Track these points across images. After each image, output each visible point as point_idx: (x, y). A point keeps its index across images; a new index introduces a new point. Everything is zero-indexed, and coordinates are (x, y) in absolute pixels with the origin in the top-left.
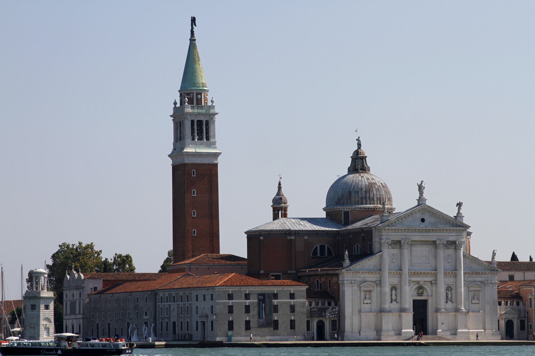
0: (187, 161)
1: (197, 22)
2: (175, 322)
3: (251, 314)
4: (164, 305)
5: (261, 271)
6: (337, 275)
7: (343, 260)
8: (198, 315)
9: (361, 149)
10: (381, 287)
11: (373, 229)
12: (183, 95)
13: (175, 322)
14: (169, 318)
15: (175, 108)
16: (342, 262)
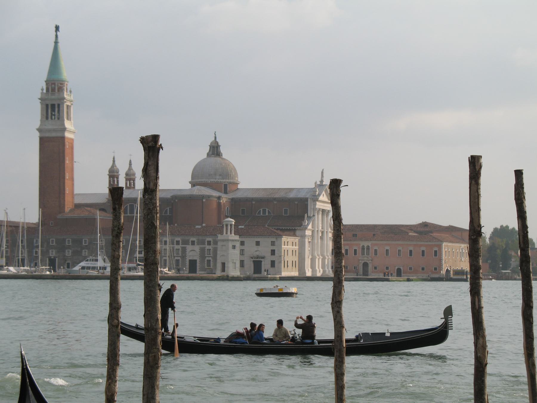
0: (67, 135)
1: (60, 29)
2: (195, 261)
3: (288, 256)
4: (174, 247)
5: (203, 224)
6: (295, 230)
7: (304, 220)
8: (245, 256)
9: (217, 140)
10: (312, 240)
11: (309, 200)
12: (56, 84)
13: (195, 261)
14: (184, 257)
15: (42, 93)
16: (302, 222)
